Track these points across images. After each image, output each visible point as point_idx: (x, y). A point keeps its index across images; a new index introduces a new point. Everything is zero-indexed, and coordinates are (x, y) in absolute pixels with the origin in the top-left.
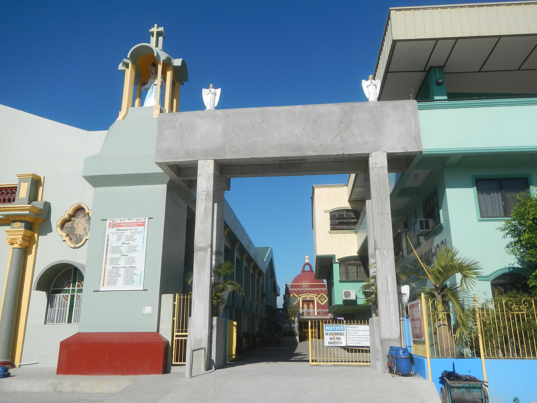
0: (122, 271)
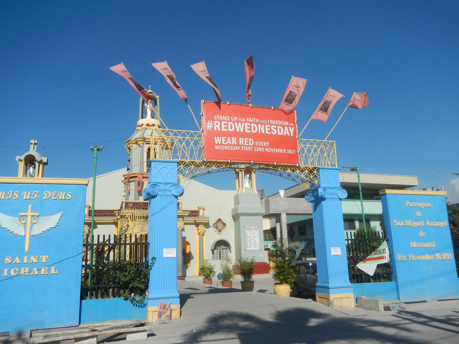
0: (252, 244)
